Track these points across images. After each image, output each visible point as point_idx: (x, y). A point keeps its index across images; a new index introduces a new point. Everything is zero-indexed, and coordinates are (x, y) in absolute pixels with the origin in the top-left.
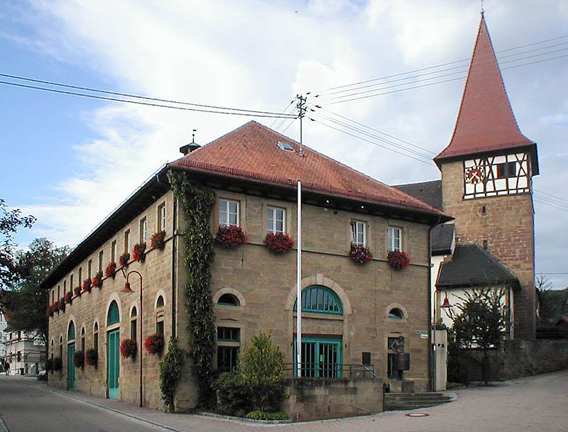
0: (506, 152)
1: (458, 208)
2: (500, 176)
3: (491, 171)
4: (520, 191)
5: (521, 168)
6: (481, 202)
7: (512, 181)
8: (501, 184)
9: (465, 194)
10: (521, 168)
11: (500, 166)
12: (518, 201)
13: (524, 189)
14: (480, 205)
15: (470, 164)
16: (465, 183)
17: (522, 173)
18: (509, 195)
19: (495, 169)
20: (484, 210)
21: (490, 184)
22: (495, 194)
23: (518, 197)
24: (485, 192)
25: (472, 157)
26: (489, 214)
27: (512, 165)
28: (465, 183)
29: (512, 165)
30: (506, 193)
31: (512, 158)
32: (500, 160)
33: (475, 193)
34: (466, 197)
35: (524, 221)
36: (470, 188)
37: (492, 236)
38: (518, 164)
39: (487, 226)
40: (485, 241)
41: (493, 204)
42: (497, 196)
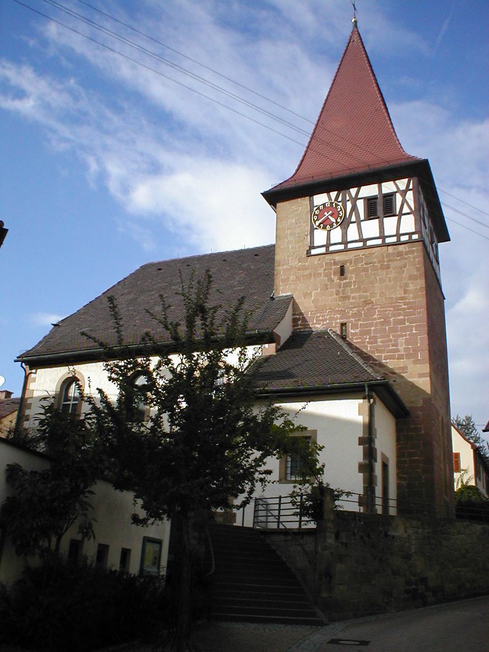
0: (377, 177)
3: (354, 208)
4: (404, 238)
5: (404, 201)
6: (337, 257)
7: (390, 224)
8: (371, 228)
9: (312, 247)
10: (404, 201)
11: (371, 202)
12: (400, 254)
13: (410, 234)
14: (335, 263)
15: (320, 199)
19: (360, 205)
20: (342, 272)
21: (352, 229)
22: (360, 244)
23: (401, 248)
24: (345, 242)
26: (351, 277)
27: (389, 199)
28: (312, 230)
29: (389, 199)
31: (388, 187)
32: (370, 190)
34: (314, 252)
36: (320, 237)
37: (357, 315)
38: (398, 195)
40: (343, 325)
41: (358, 260)
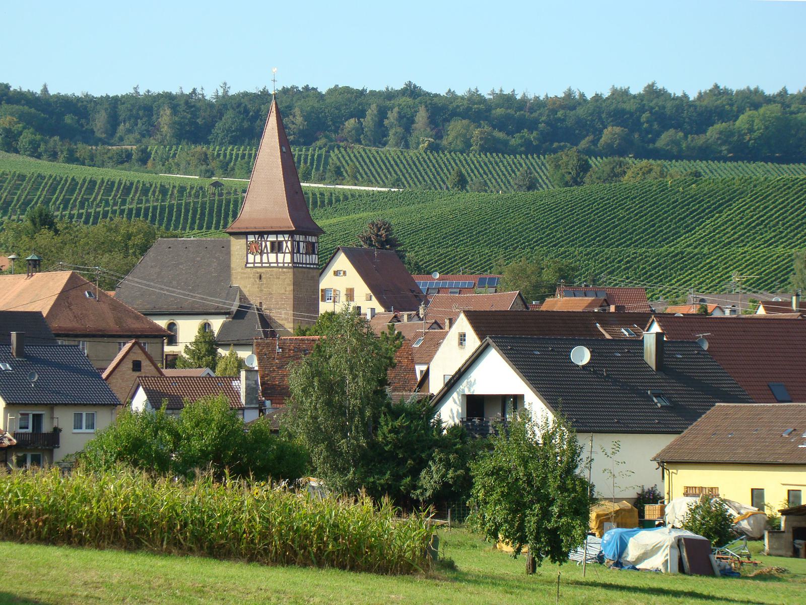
0: (277, 233)
1: (242, 273)
2: (272, 251)
3: (266, 246)
4: (286, 265)
5: (287, 246)
6: (259, 270)
7: (280, 256)
8: (272, 257)
9: (247, 263)
10: (287, 246)
11: (272, 243)
12: (284, 272)
13: (289, 263)
14: (257, 273)
15: (251, 238)
16: (247, 254)
17: (287, 251)
18: (278, 267)
19: (268, 244)
20: (260, 277)
21: (265, 256)
22: (268, 265)
23: (285, 270)
24: (261, 262)
25: (254, 233)
26: (264, 281)
27: (280, 243)
28: (247, 254)
29: (280, 243)
30: (276, 265)
31: (281, 238)
32: (272, 238)
33: (254, 263)
34: (248, 265)
35: (288, 289)
36: (251, 258)
37: (266, 299)
38: (284, 242)
39: (261, 291)
40: (261, 303)
41: (267, 272)
42: (270, 267)
